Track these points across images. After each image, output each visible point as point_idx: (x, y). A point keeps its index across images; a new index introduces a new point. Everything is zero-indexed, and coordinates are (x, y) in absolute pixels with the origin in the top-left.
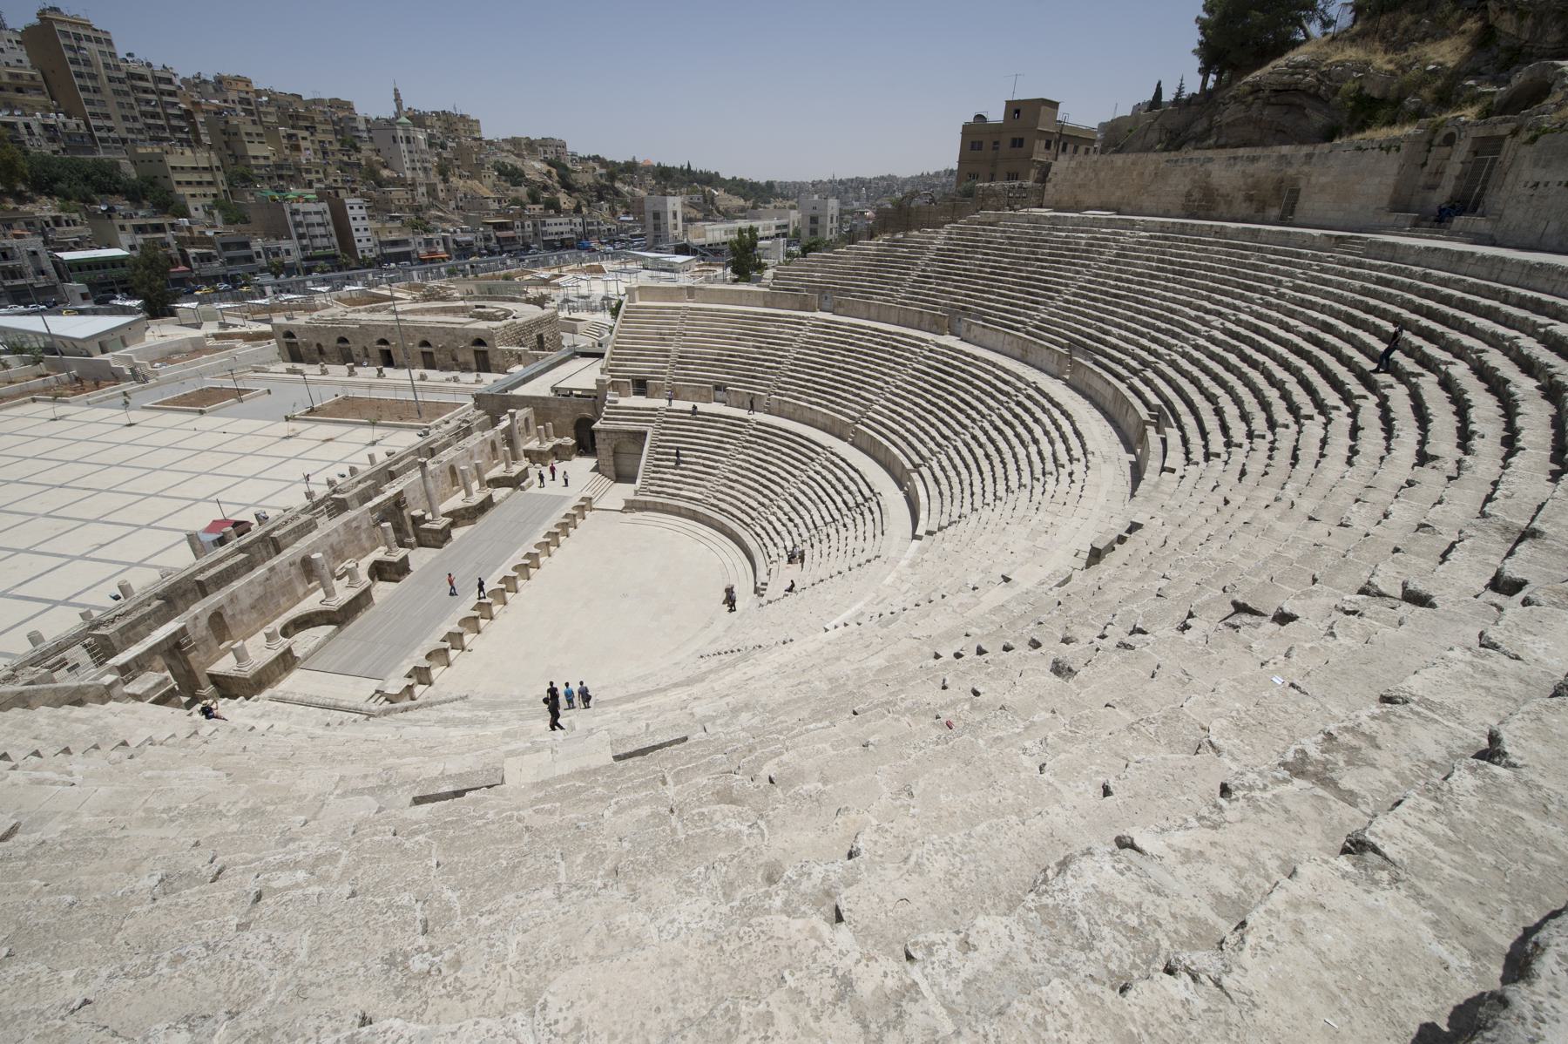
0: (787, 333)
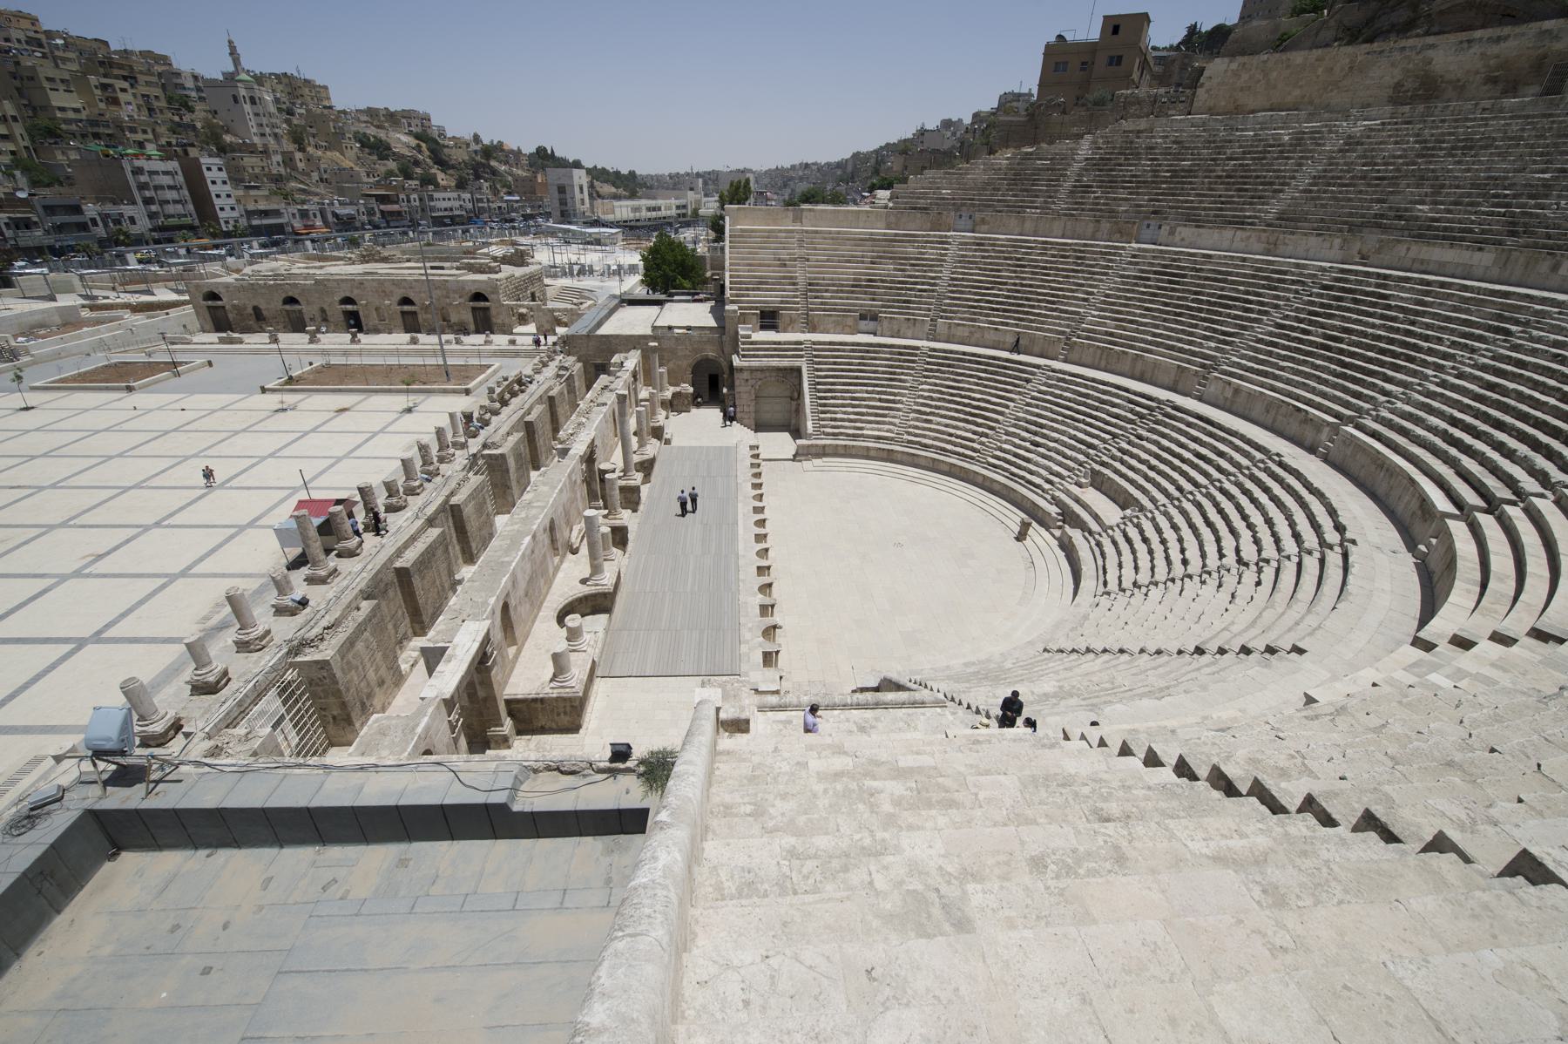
0: (931, 253)
